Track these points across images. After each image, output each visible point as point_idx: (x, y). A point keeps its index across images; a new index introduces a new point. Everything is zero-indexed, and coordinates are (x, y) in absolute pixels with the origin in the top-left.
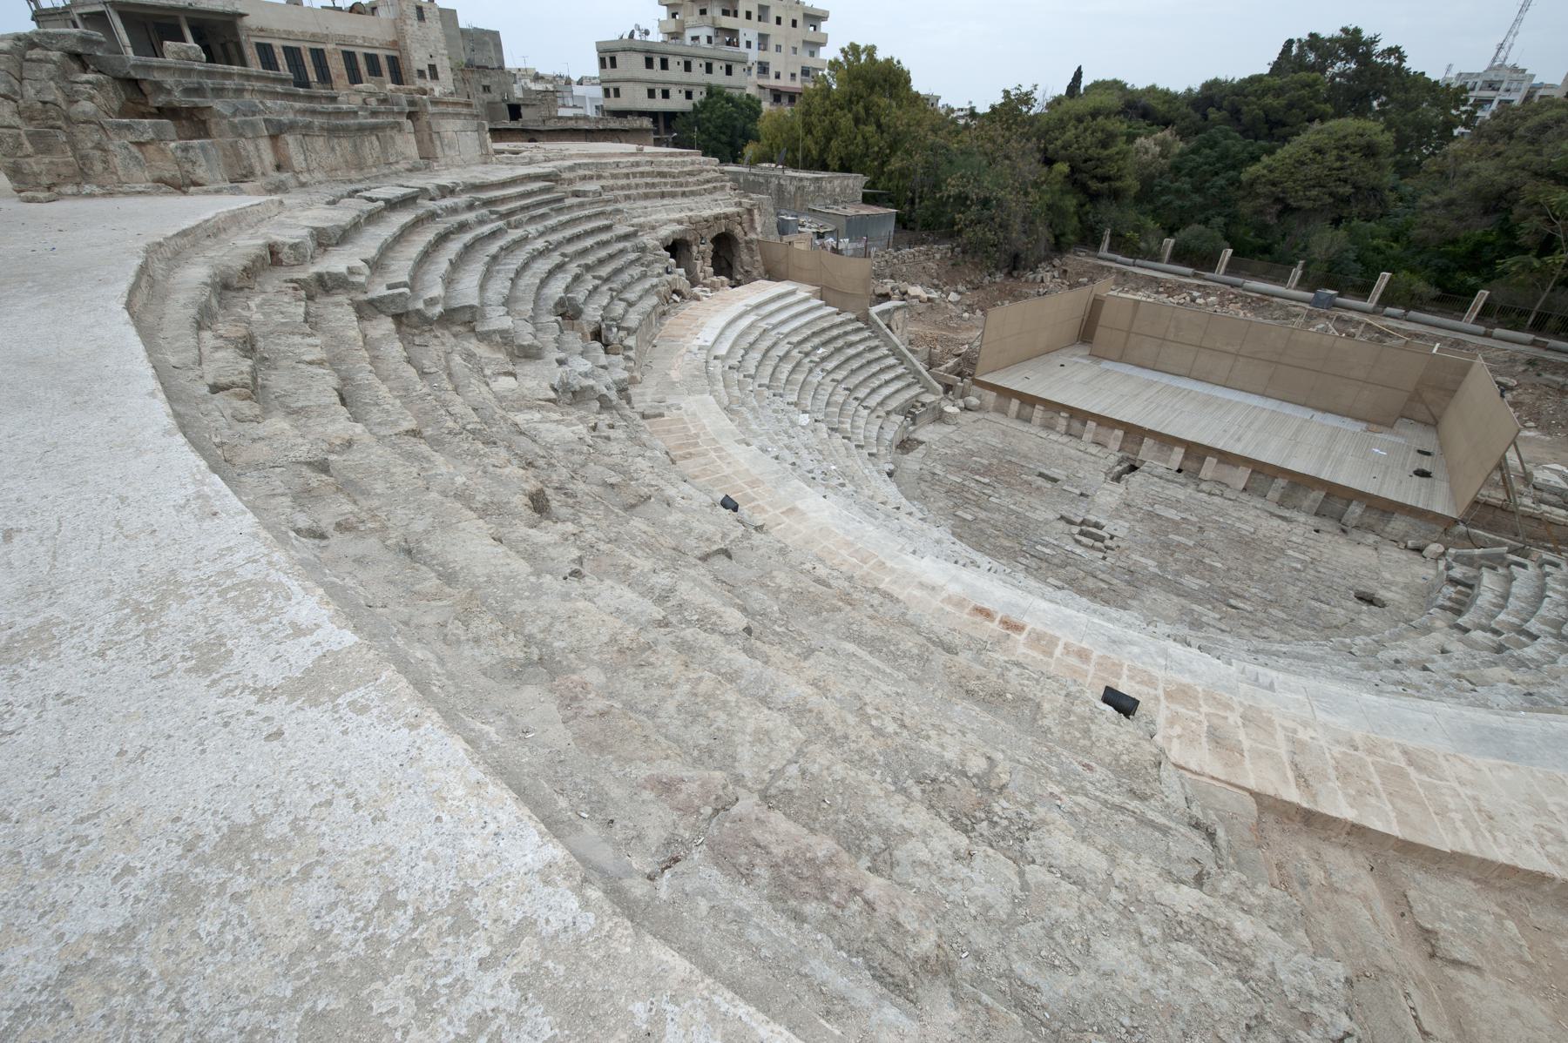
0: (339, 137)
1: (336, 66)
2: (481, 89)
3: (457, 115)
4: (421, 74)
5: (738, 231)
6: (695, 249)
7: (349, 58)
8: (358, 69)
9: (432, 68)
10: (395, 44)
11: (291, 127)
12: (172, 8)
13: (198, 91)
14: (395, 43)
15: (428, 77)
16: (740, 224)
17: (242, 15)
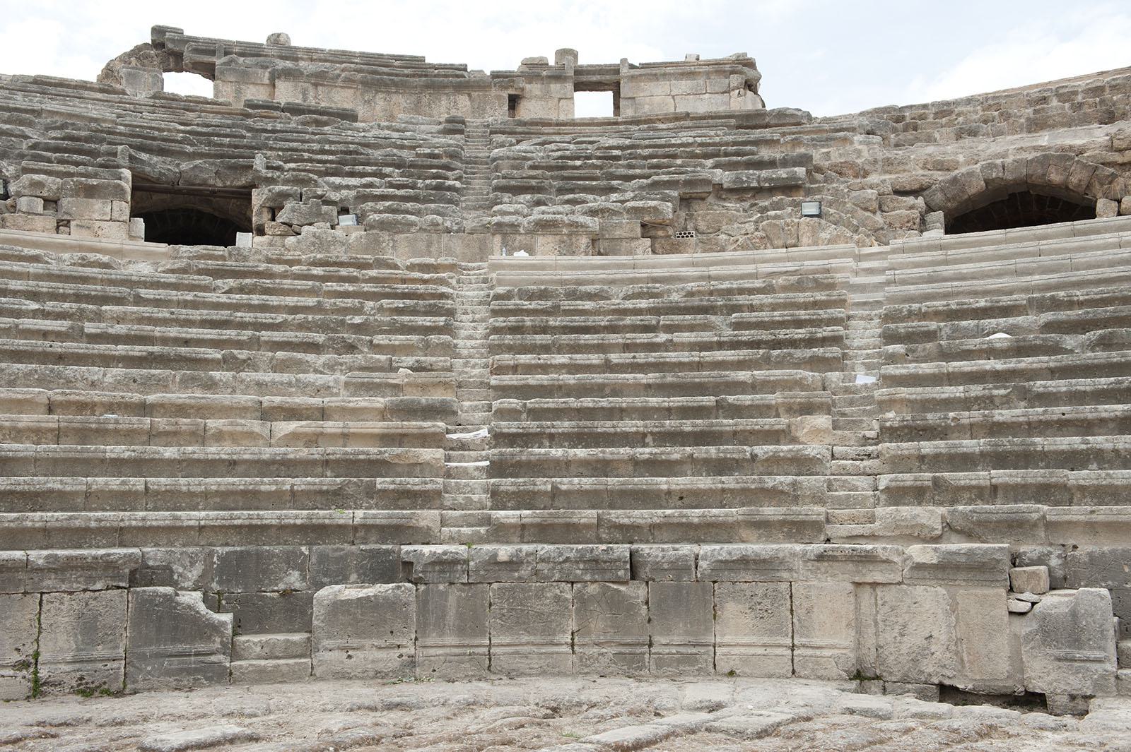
0: (389, 93)
11: (288, 74)
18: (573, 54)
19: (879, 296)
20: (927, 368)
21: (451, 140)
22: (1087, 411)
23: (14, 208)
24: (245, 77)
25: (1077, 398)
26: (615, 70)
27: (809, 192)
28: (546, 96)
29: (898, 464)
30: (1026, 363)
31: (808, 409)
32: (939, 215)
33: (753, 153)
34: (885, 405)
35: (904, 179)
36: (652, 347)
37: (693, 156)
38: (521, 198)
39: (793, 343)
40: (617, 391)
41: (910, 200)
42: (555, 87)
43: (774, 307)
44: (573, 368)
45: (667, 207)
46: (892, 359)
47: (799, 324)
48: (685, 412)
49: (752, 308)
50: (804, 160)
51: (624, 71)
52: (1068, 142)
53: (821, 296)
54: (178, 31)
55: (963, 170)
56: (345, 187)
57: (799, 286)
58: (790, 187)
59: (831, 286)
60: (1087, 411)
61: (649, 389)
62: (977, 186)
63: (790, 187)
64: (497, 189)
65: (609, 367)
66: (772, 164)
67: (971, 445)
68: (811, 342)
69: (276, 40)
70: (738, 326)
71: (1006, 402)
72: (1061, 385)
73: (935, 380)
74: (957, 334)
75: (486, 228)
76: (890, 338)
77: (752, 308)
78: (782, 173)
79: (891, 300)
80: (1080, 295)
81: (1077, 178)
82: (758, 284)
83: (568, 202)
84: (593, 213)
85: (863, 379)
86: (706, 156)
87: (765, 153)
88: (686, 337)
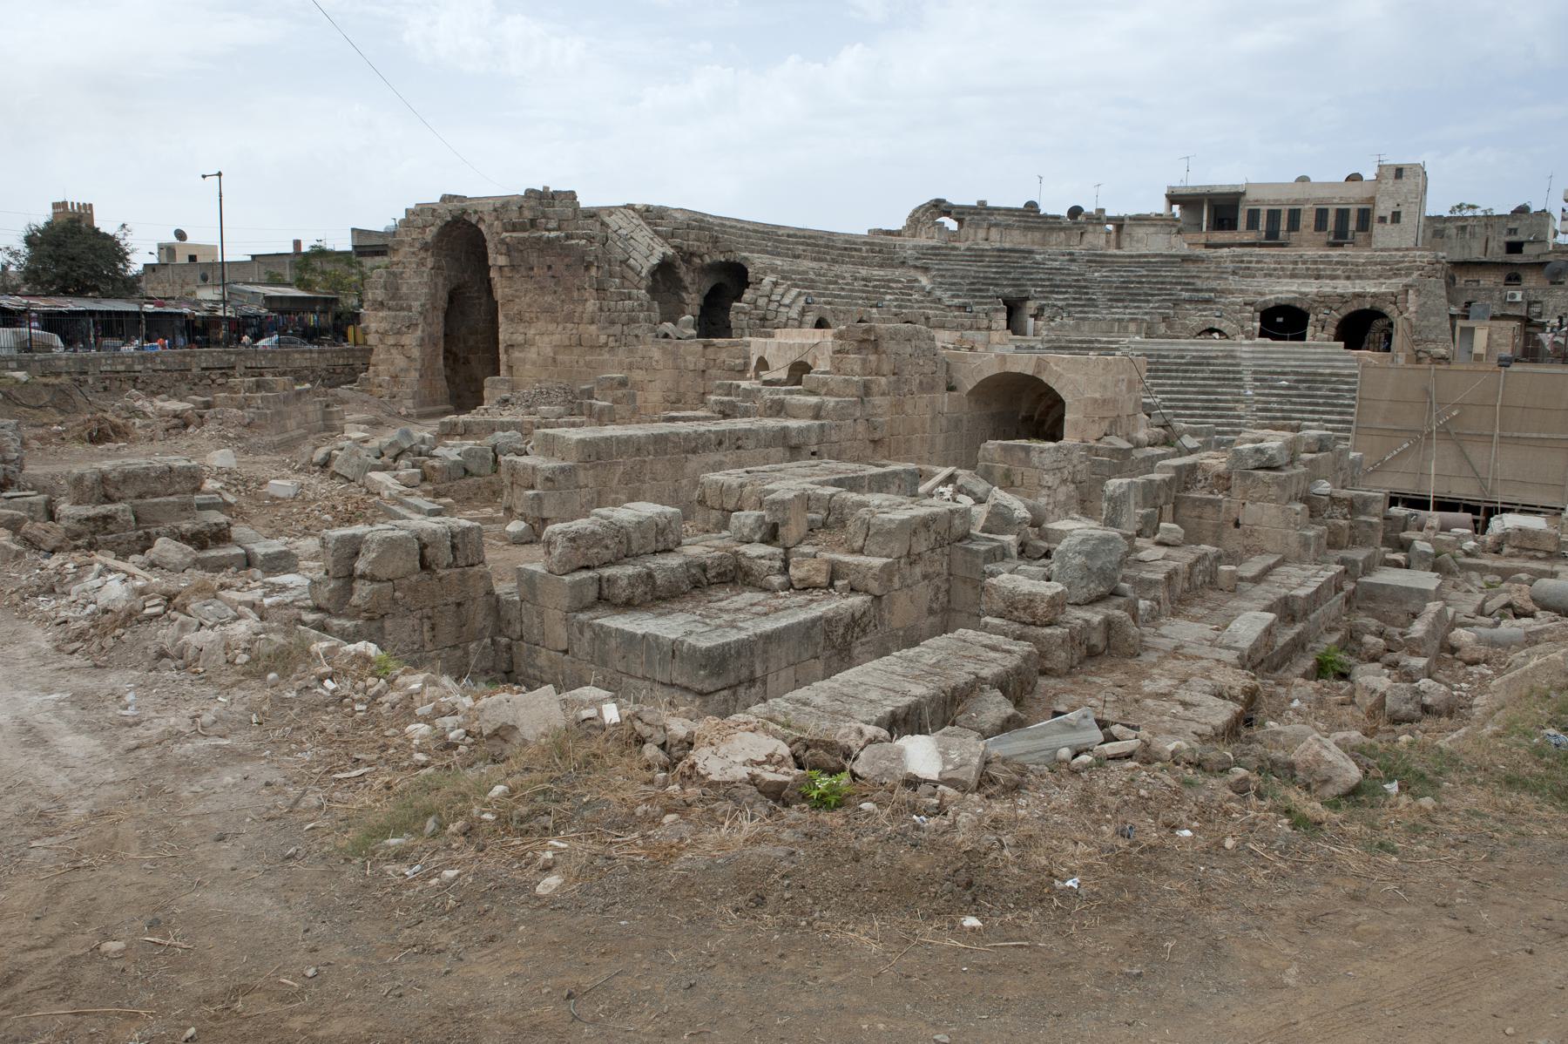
1: (1308, 219)
2: (1505, 232)
3: (1155, 225)
4: (1383, 220)
5: (1389, 309)
6: (1312, 318)
7: (1321, 215)
8: (1326, 221)
9: (1396, 217)
10: (1372, 200)
11: (996, 225)
12: (1198, 195)
13: (963, 213)
14: (1373, 198)
15: (1389, 221)
16: (1395, 303)
17: (1243, 194)
18: (1102, 211)
19: (1248, 363)
20: (1267, 391)
21: (1074, 267)
22: (1303, 408)
23: (975, 317)
24: (978, 226)
25: (1301, 404)
26: (1122, 219)
27: (1215, 303)
28: (1095, 231)
29: (1262, 418)
30: (1291, 392)
31: (1237, 401)
32: (1258, 314)
33: (1193, 284)
34: (1257, 402)
35: (1248, 299)
36: (1190, 378)
37: (1171, 283)
38: (1120, 304)
39: (1228, 379)
40: (1186, 393)
41: (1248, 308)
42: (1098, 228)
43: (1220, 365)
44: (1172, 385)
45: (1172, 312)
46: (1256, 387)
47: (1229, 372)
48: (1207, 401)
49: (1214, 365)
50: (1212, 290)
51: (1127, 221)
52: (1303, 289)
53: (1233, 362)
54: (944, 201)
55: (1268, 298)
56: (1058, 299)
57: (1225, 357)
58: (1208, 301)
59: (1234, 357)
60: (1303, 408)
61: (1194, 393)
62: (1272, 305)
63: (1208, 301)
64: (1110, 300)
65: (1182, 385)
66: (1202, 290)
67: (1279, 415)
68: (1234, 379)
69: (982, 204)
70: (1212, 372)
71: (1285, 404)
72: (1298, 400)
73: (1267, 395)
74: (1272, 380)
75: (1114, 320)
76: (1256, 380)
77: (1214, 365)
78: (1206, 295)
79: (1255, 365)
80: (1304, 370)
81: (1305, 307)
82: (1213, 354)
83: (1136, 307)
84: (1146, 313)
85: (1250, 393)
86: (1177, 283)
87: (1199, 283)
88: (1200, 375)
